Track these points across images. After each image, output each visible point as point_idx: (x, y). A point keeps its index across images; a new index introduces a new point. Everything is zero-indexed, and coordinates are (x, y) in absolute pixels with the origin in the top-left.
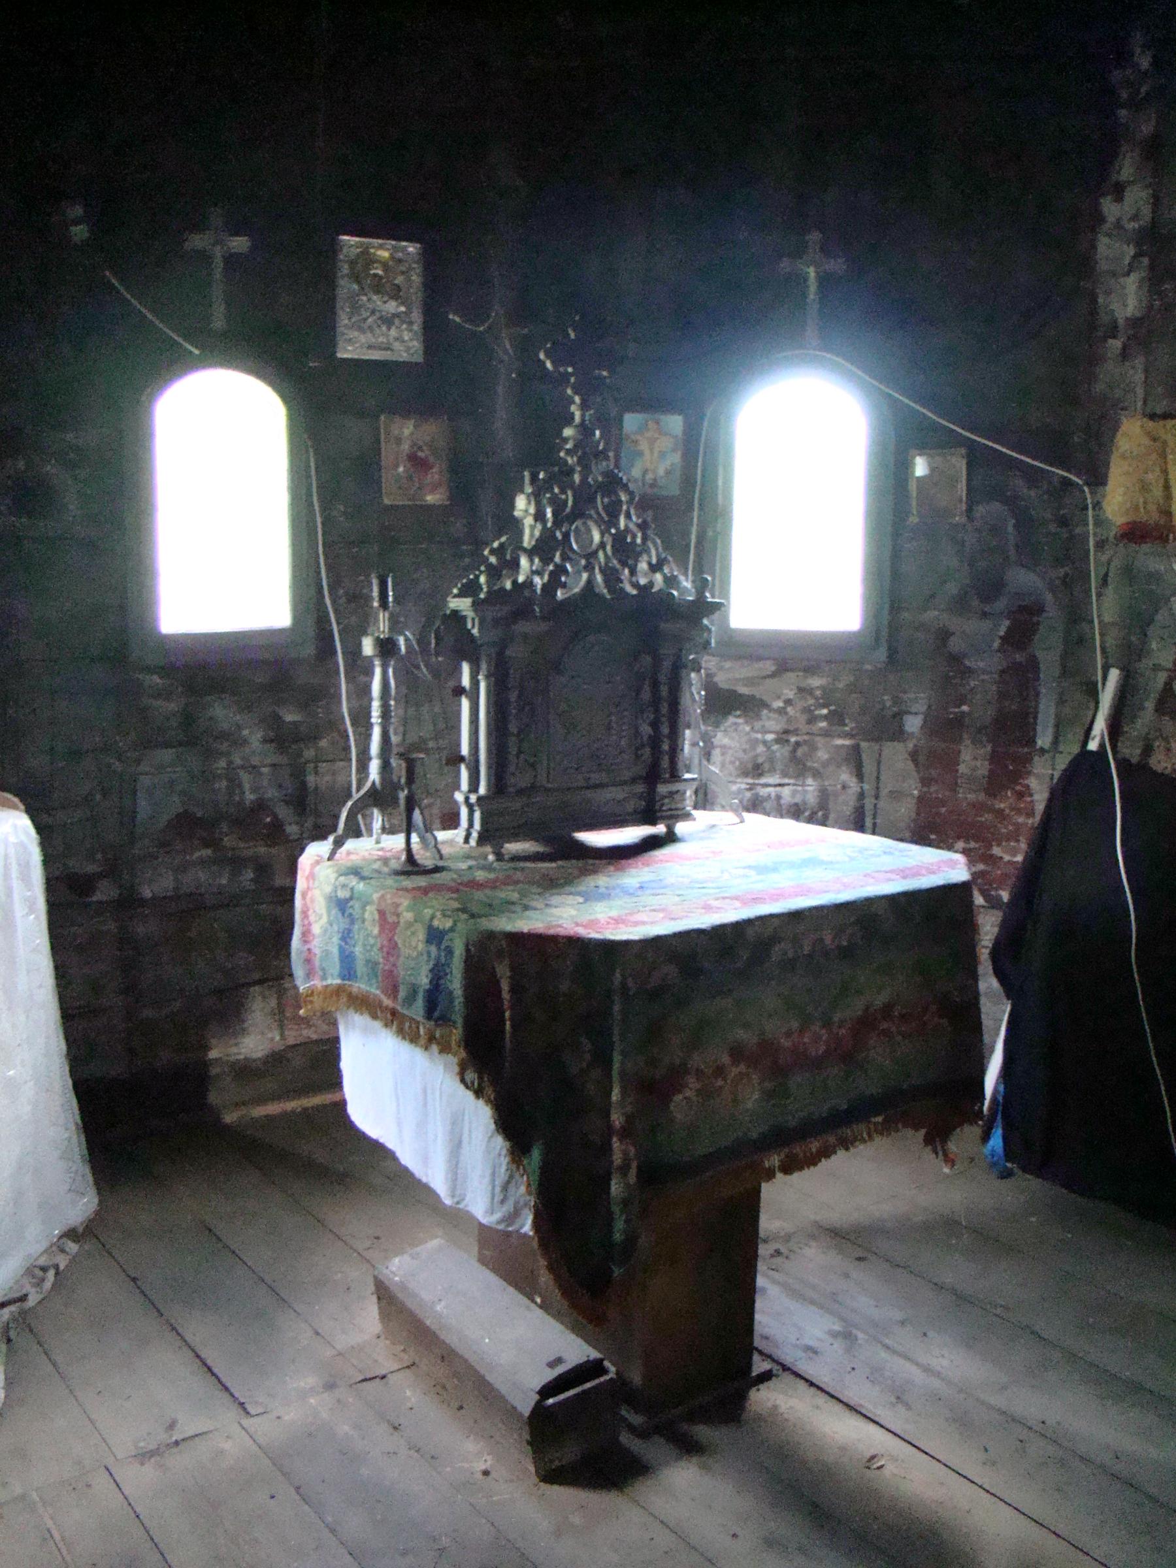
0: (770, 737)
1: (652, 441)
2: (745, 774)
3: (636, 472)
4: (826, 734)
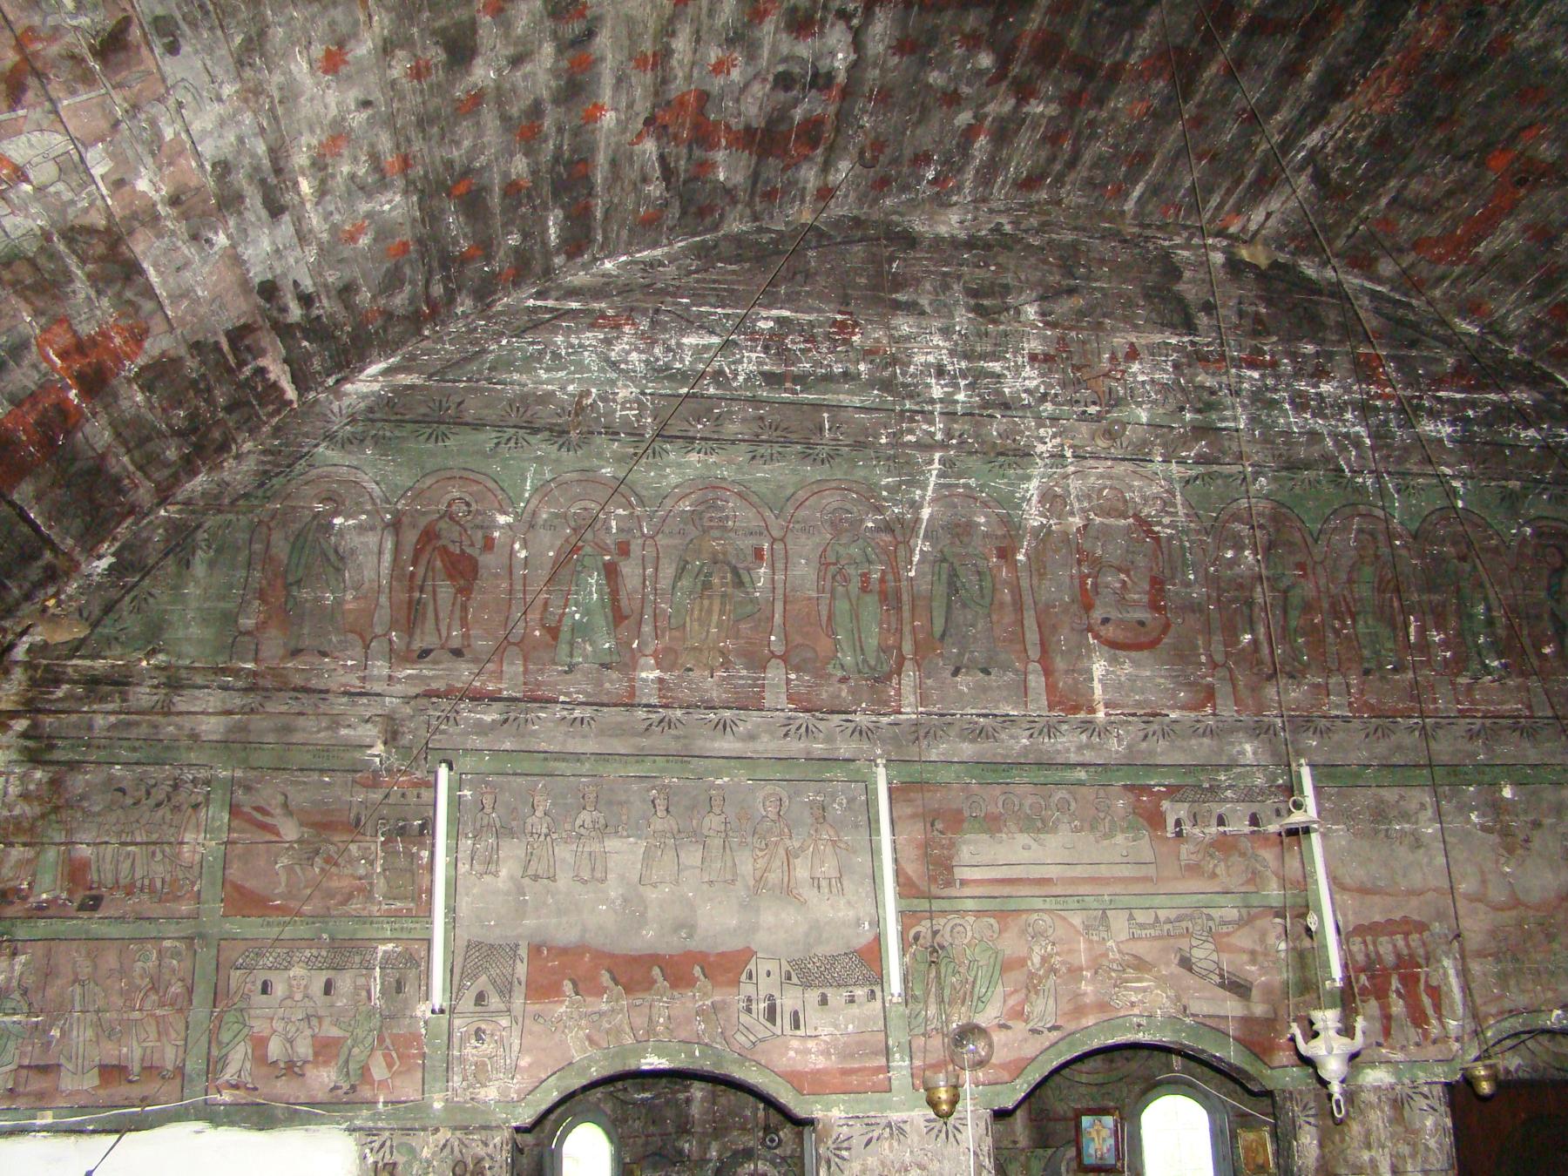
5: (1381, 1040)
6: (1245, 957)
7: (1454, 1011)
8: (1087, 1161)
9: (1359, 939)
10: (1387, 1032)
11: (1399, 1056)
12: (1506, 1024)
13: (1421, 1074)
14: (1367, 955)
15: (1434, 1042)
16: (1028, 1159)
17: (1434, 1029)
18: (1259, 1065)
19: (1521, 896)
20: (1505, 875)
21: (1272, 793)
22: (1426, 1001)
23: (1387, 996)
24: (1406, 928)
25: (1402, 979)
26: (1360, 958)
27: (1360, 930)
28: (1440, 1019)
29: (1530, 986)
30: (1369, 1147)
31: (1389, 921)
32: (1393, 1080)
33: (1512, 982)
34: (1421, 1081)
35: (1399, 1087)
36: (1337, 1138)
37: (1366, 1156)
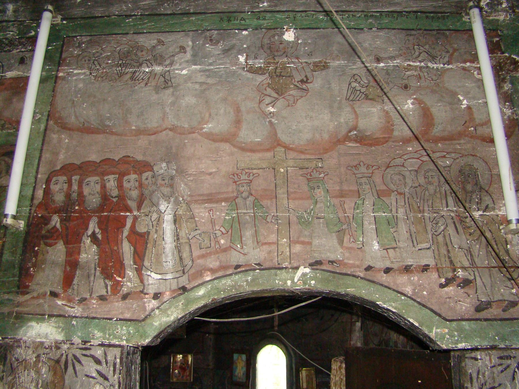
5: (59, 290)
7: (159, 261)
9: (65, 178)
11: (77, 310)
12: (228, 282)
13: (98, 334)
14: (68, 196)
15: (125, 297)
19: (283, 138)
20: (265, 115)
21: (21, 44)
23: (79, 240)
24: (123, 168)
25: (103, 224)
26: (59, 198)
28: (139, 271)
31: (106, 161)
32: (60, 337)
33: (248, 233)
34: (97, 342)
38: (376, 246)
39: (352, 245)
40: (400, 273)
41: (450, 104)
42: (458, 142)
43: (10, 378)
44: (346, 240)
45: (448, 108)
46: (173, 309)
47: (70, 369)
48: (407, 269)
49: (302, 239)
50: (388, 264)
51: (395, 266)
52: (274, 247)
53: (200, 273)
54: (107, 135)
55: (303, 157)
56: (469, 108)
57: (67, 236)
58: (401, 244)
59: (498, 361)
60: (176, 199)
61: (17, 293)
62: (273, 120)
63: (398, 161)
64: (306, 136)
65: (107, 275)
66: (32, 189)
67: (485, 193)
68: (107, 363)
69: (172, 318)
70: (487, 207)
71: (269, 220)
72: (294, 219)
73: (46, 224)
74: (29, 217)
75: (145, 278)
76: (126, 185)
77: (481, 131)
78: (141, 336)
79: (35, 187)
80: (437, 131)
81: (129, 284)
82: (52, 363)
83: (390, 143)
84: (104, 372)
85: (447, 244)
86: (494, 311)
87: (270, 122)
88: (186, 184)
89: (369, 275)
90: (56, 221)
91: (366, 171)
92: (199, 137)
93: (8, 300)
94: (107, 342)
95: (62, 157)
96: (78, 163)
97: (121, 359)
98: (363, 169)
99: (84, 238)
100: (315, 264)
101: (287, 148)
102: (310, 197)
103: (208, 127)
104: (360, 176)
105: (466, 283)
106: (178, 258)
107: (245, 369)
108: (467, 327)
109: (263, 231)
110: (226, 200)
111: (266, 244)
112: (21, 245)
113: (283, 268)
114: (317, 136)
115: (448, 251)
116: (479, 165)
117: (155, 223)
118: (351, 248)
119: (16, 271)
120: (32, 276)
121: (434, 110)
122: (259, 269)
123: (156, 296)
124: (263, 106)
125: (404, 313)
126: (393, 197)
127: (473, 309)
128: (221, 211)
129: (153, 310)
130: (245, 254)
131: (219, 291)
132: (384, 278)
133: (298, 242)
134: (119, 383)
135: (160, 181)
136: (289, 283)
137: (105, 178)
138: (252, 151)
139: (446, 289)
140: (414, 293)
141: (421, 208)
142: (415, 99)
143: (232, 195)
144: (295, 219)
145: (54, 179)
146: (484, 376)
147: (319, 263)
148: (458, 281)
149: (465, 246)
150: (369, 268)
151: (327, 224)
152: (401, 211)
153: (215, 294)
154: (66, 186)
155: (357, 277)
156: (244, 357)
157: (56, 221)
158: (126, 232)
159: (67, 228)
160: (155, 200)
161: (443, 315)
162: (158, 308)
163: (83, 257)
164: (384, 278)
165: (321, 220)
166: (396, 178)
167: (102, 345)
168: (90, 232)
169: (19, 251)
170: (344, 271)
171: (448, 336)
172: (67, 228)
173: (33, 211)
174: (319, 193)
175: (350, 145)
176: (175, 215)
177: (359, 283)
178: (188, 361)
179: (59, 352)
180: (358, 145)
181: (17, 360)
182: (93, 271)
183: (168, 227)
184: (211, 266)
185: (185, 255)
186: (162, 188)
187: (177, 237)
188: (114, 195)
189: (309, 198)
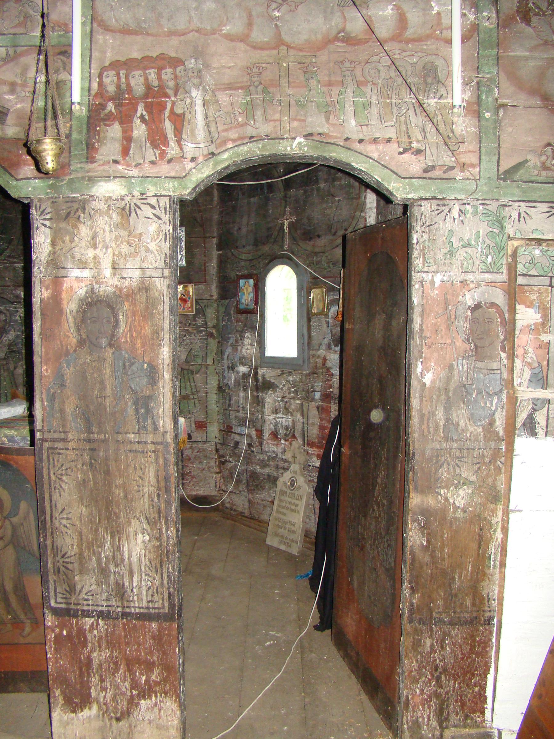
0: (279, 399)
1: (247, 289)
2: (273, 413)
3: (243, 301)
4: (294, 398)
5: (119, 158)
6: (5, 88)
7: (193, 135)
8: (241, 307)
9: (114, 73)
10: (125, 152)
11: (135, 172)
12: (245, 148)
14: (118, 87)
15: (170, 161)
16: (218, 305)
17: (172, 150)
18: (7, 177)
19: (286, 38)
20: (273, 19)
22: (168, 126)
24: (160, 63)
25: (149, 107)
26: (111, 89)
27: (115, 65)
28: (179, 142)
29: (277, 116)
30: (95, 247)
32: (124, 192)
33: (259, 113)
34: (151, 194)
35: (128, 199)
36: (68, 238)
37: (91, 253)
38: (353, 123)
39: (336, 122)
40: (370, 143)
41: (424, 10)
42: (425, 43)
43: (90, 223)
44: (331, 117)
45: (421, 13)
46: (205, 168)
47: (133, 213)
48: (375, 141)
49: (299, 117)
50: (361, 137)
51: (366, 138)
52: (278, 123)
53: (224, 143)
54: (145, 36)
55: (301, 54)
56: (439, 14)
57: (121, 118)
58: (372, 122)
59: (436, 208)
60: (204, 87)
61: (87, 162)
62: (278, 23)
63: (376, 58)
64: (304, 37)
65: (155, 145)
66: (87, 82)
67: (442, 85)
68: (159, 208)
69: (205, 175)
70: (442, 96)
71: (274, 103)
72: (293, 102)
73: (103, 110)
74: (89, 104)
75: (184, 147)
76: (163, 77)
77: (445, 34)
78: (183, 188)
79: (90, 81)
80: (409, 33)
81: (172, 152)
82: (120, 210)
83: (370, 44)
84: (158, 214)
85: (407, 123)
86: (437, 173)
87: (276, 25)
88: (211, 76)
89: (347, 144)
90: (111, 107)
91: (349, 66)
92: (220, 38)
93: (81, 168)
94: (159, 193)
95: (109, 55)
96: (123, 59)
97: (170, 205)
98: (347, 64)
99: (135, 119)
100: (308, 136)
101: (289, 47)
102: (307, 86)
103: (226, 29)
104: (345, 69)
105: (418, 152)
106: (207, 132)
107: (252, 295)
108: (416, 183)
109: (270, 112)
110: (241, 88)
111: (272, 121)
112: (85, 126)
113: (284, 139)
114: (313, 37)
115: (407, 128)
116: (439, 63)
117: (188, 106)
118: (335, 124)
119: (84, 146)
120: (97, 150)
121: (409, 16)
122: (268, 139)
123: (193, 160)
124: (270, 11)
125: (370, 171)
126: (369, 86)
127: (421, 171)
128: (239, 96)
129: (191, 170)
130: (256, 129)
131: (238, 155)
132: (358, 147)
133: (296, 120)
134: (170, 221)
135: (190, 74)
136: (289, 149)
137: (147, 72)
138: (262, 49)
139: (403, 156)
140: (379, 158)
141: (390, 96)
142: (394, 5)
143: (246, 84)
144: (294, 102)
145: (105, 73)
146: (425, 217)
147: (311, 135)
148: (413, 150)
149: (420, 125)
150: (347, 139)
151: (318, 107)
152: (374, 98)
153: (235, 157)
154: (115, 79)
155: (338, 145)
156: (251, 282)
157: (111, 107)
158: (167, 114)
159: (121, 112)
160: (187, 88)
161: (399, 174)
162: (194, 168)
163: (135, 133)
164: (358, 147)
165: (313, 104)
166: (373, 71)
167: (155, 196)
168: (139, 114)
169: (85, 131)
170: (329, 141)
171: (401, 189)
172: (121, 112)
173: (91, 100)
174: (313, 83)
175: (339, 44)
176: (204, 100)
177: (339, 149)
178: (189, 292)
179: (124, 203)
180: (344, 44)
181: (94, 210)
182: (144, 144)
183: (199, 109)
184: (232, 137)
185: (213, 129)
186: (193, 79)
187: (206, 117)
188: (155, 85)
189: (305, 87)
